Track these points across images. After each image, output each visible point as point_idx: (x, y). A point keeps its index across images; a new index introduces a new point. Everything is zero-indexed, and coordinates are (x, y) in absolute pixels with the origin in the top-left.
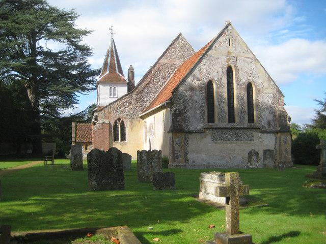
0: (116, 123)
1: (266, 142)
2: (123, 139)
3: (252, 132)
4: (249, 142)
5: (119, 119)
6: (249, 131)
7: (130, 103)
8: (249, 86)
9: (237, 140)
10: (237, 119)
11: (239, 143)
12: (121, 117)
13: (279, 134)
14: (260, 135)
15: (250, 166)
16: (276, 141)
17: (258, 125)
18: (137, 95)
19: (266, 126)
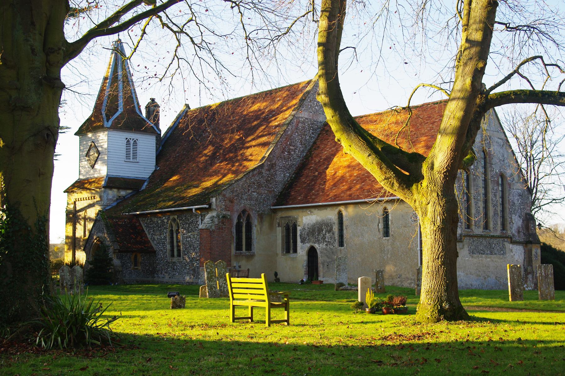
0: (239, 217)
1: (516, 257)
2: (249, 246)
3: (506, 244)
4: (501, 256)
5: (244, 211)
6: (501, 239)
7: (260, 186)
8: (502, 176)
9: (491, 253)
10: (491, 225)
11: (493, 256)
12: (248, 207)
13: (529, 246)
14: (511, 246)
15: (526, 289)
16: (525, 255)
17: (509, 233)
18: (269, 170)
19: (516, 234)
